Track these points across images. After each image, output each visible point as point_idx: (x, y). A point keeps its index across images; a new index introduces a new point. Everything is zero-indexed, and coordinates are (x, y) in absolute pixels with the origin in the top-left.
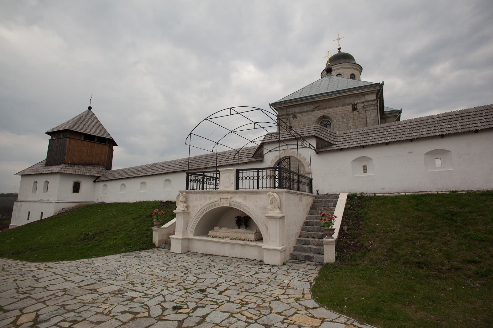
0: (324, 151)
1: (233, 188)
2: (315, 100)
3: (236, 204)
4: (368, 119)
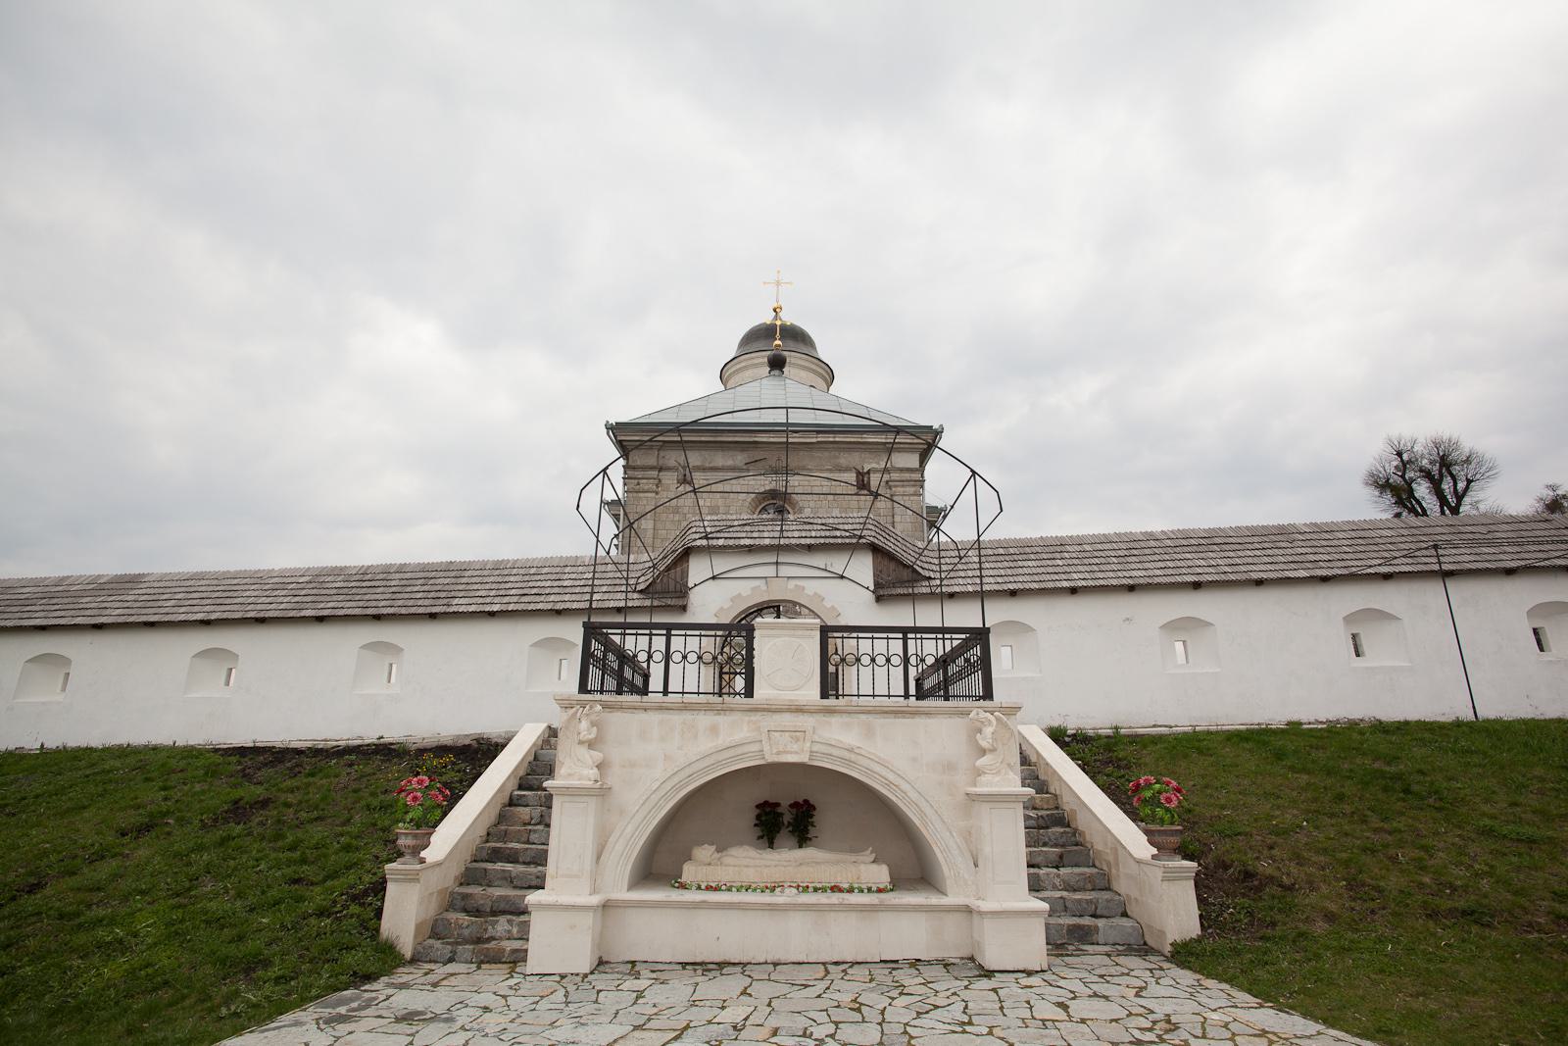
0: (905, 595)
1: (812, 692)
2: (756, 439)
3: (835, 752)
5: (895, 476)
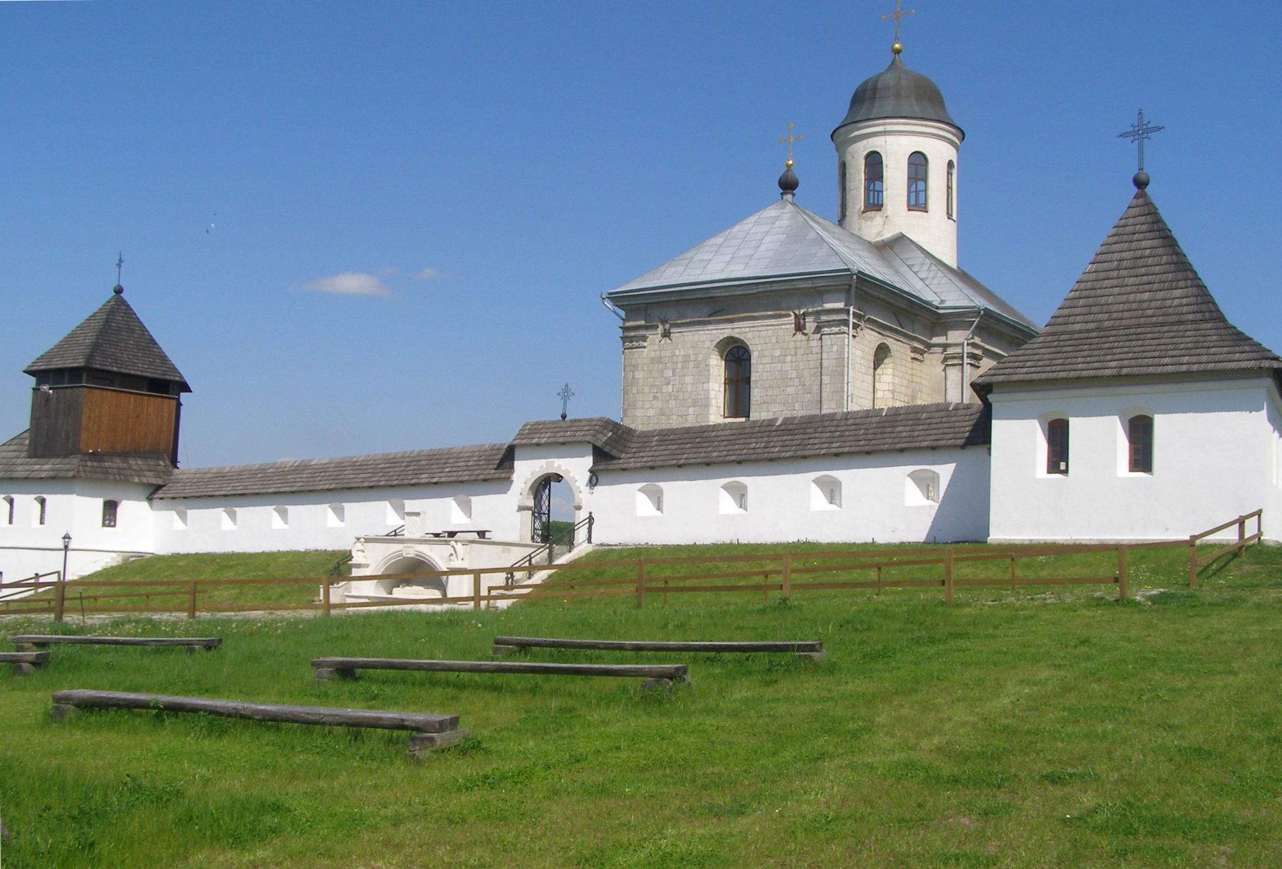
4: (825, 356)
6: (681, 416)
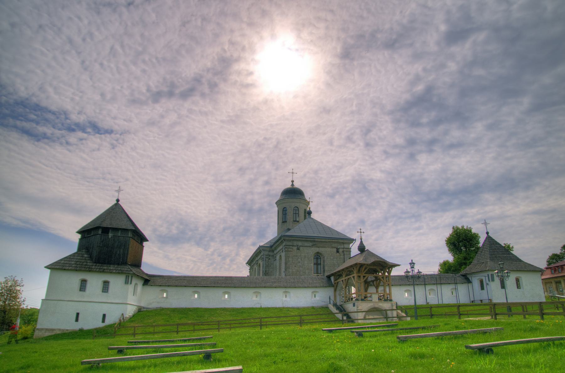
1: (376, 292)
5: (345, 250)
6: (304, 272)
